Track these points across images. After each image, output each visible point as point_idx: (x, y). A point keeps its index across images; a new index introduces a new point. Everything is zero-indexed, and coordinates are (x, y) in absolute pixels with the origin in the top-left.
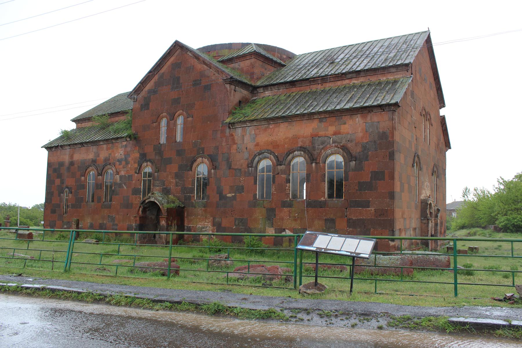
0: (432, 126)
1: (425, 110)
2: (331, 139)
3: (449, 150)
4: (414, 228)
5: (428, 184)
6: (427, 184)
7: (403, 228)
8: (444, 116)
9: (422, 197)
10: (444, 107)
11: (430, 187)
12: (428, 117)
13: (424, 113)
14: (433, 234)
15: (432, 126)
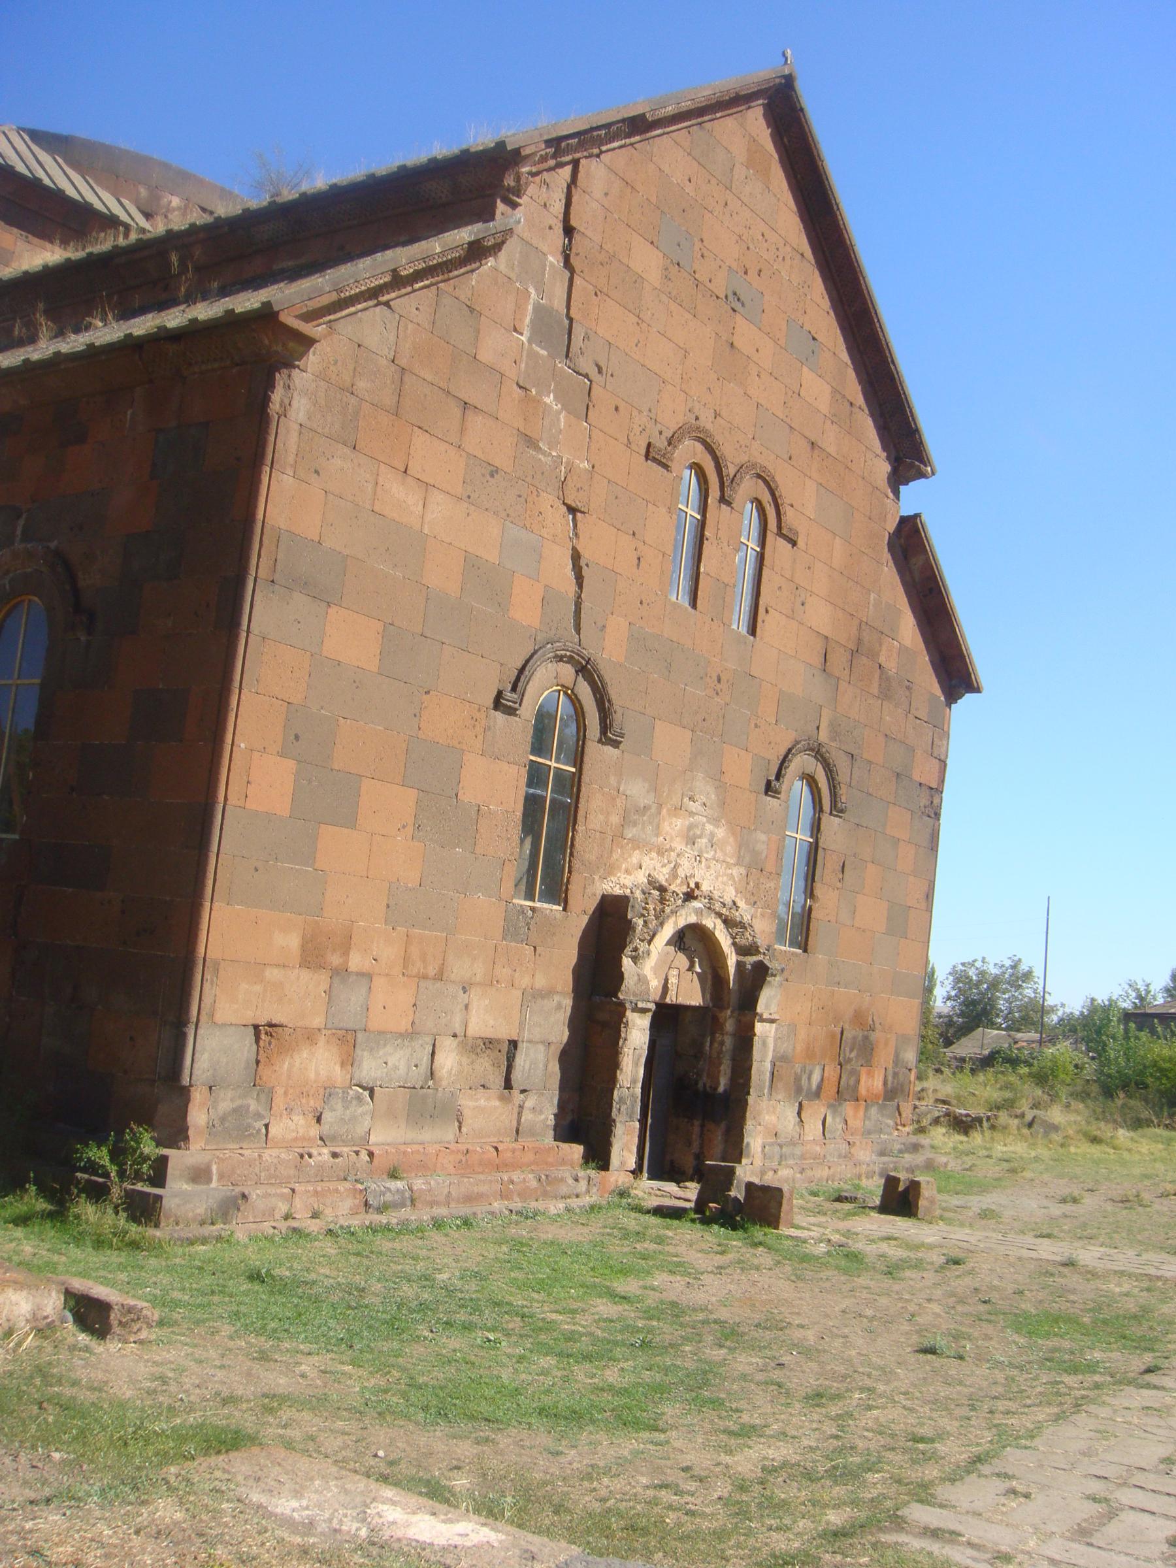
0: (794, 543)
1: (710, 449)
2: (22, 522)
3: (969, 697)
4: (489, 1043)
5: (720, 833)
6: (691, 827)
7: (317, 1021)
8: (917, 515)
9: (613, 886)
10: (922, 475)
11: (729, 849)
12: (748, 487)
13: (689, 450)
14: (721, 1089)
15: (794, 543)
